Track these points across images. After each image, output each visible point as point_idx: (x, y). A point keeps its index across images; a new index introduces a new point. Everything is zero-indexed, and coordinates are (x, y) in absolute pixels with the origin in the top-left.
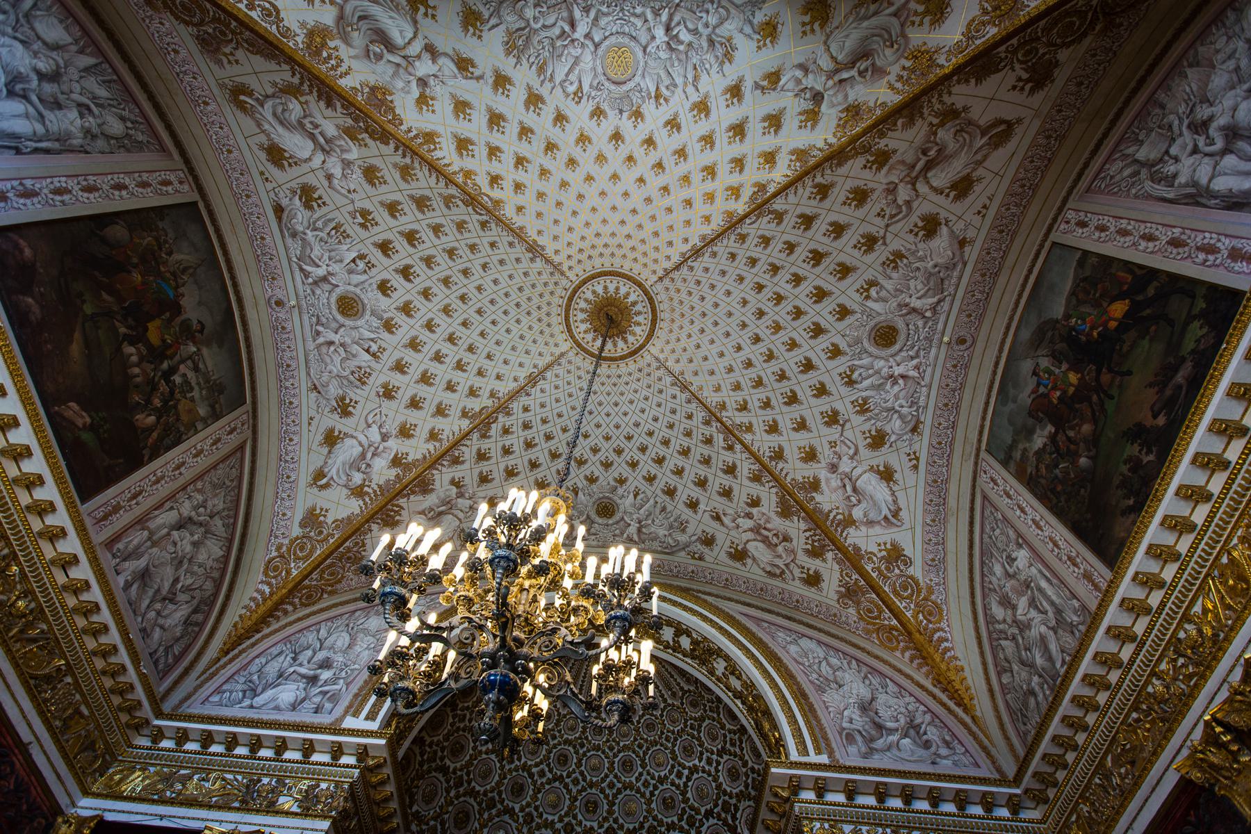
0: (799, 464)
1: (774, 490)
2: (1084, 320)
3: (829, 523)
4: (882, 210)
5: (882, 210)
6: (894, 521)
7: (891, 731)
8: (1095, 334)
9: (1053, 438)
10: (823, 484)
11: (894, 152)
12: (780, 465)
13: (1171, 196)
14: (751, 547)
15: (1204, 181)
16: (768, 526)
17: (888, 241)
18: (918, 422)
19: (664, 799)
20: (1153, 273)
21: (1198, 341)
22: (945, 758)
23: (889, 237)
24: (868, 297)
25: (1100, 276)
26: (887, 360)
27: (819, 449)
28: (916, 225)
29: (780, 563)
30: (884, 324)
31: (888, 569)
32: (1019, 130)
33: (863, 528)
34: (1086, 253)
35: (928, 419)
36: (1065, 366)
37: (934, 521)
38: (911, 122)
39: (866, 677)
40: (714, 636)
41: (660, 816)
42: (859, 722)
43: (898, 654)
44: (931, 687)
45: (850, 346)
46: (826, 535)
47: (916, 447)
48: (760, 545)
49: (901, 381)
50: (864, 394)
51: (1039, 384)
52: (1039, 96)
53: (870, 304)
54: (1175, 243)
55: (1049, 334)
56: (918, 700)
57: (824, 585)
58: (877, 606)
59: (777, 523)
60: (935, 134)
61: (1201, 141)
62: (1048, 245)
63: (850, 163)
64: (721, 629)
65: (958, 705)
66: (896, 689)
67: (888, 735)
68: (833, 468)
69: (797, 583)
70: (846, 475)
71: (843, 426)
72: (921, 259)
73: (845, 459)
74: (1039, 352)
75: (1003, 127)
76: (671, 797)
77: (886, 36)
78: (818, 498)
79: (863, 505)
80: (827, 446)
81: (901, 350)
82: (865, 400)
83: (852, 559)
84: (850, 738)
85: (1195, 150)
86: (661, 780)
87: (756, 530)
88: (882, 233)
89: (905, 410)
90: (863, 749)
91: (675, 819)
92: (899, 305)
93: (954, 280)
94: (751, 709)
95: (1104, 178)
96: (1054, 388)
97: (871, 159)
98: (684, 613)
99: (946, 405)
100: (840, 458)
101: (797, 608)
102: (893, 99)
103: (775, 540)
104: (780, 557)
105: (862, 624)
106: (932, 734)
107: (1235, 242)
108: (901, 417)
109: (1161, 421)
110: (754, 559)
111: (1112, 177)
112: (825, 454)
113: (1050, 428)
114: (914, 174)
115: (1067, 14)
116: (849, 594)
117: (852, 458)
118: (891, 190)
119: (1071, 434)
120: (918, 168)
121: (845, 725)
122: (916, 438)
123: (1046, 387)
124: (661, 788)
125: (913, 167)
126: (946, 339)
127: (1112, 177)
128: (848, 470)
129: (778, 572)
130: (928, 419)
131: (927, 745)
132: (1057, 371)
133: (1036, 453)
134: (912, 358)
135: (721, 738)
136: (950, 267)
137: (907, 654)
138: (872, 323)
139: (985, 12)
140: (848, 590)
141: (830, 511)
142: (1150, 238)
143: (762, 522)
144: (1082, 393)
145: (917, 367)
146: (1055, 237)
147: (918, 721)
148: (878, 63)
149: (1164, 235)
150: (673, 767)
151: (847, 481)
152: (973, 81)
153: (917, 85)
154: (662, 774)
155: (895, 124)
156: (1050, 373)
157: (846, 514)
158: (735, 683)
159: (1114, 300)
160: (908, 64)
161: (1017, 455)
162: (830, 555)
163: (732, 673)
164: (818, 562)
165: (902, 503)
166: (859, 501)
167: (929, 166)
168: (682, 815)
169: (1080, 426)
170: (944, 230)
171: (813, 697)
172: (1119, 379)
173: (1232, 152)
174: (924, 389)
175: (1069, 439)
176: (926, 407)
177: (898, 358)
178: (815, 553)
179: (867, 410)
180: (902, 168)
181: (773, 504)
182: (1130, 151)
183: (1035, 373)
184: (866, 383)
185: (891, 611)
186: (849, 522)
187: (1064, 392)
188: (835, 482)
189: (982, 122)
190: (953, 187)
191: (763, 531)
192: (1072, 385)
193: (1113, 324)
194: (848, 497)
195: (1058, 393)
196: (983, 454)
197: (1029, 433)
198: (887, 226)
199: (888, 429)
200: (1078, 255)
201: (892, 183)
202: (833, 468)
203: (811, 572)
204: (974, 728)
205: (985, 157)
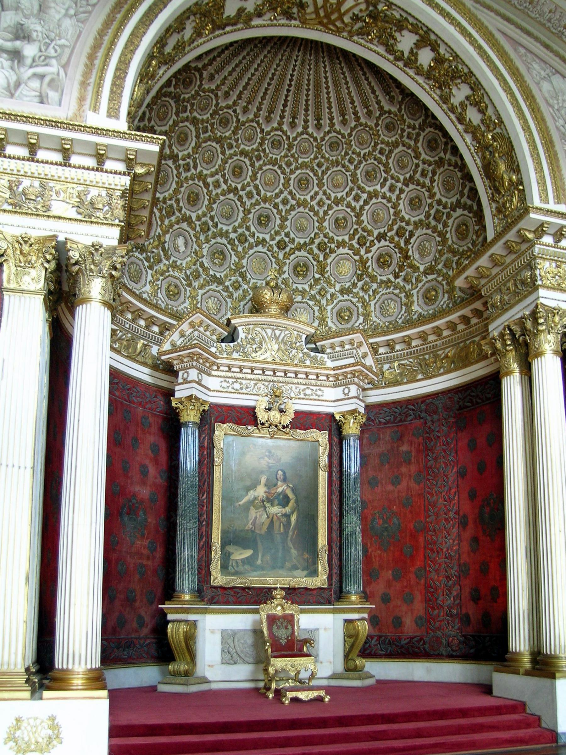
19: (337, 220)
40: (471, 58)
41: (331, 234)
64: (479, 48)
76: (345, 219)
86: (337, 202)
91: (346, 238)
94: (483, 147)
98: (440, 19)
124: (336, 208)
135: (411, 166)
150: (352, 189)
154: (339, 195)
158: (473, 115)
163: (476, 104)
168: (354, 235)
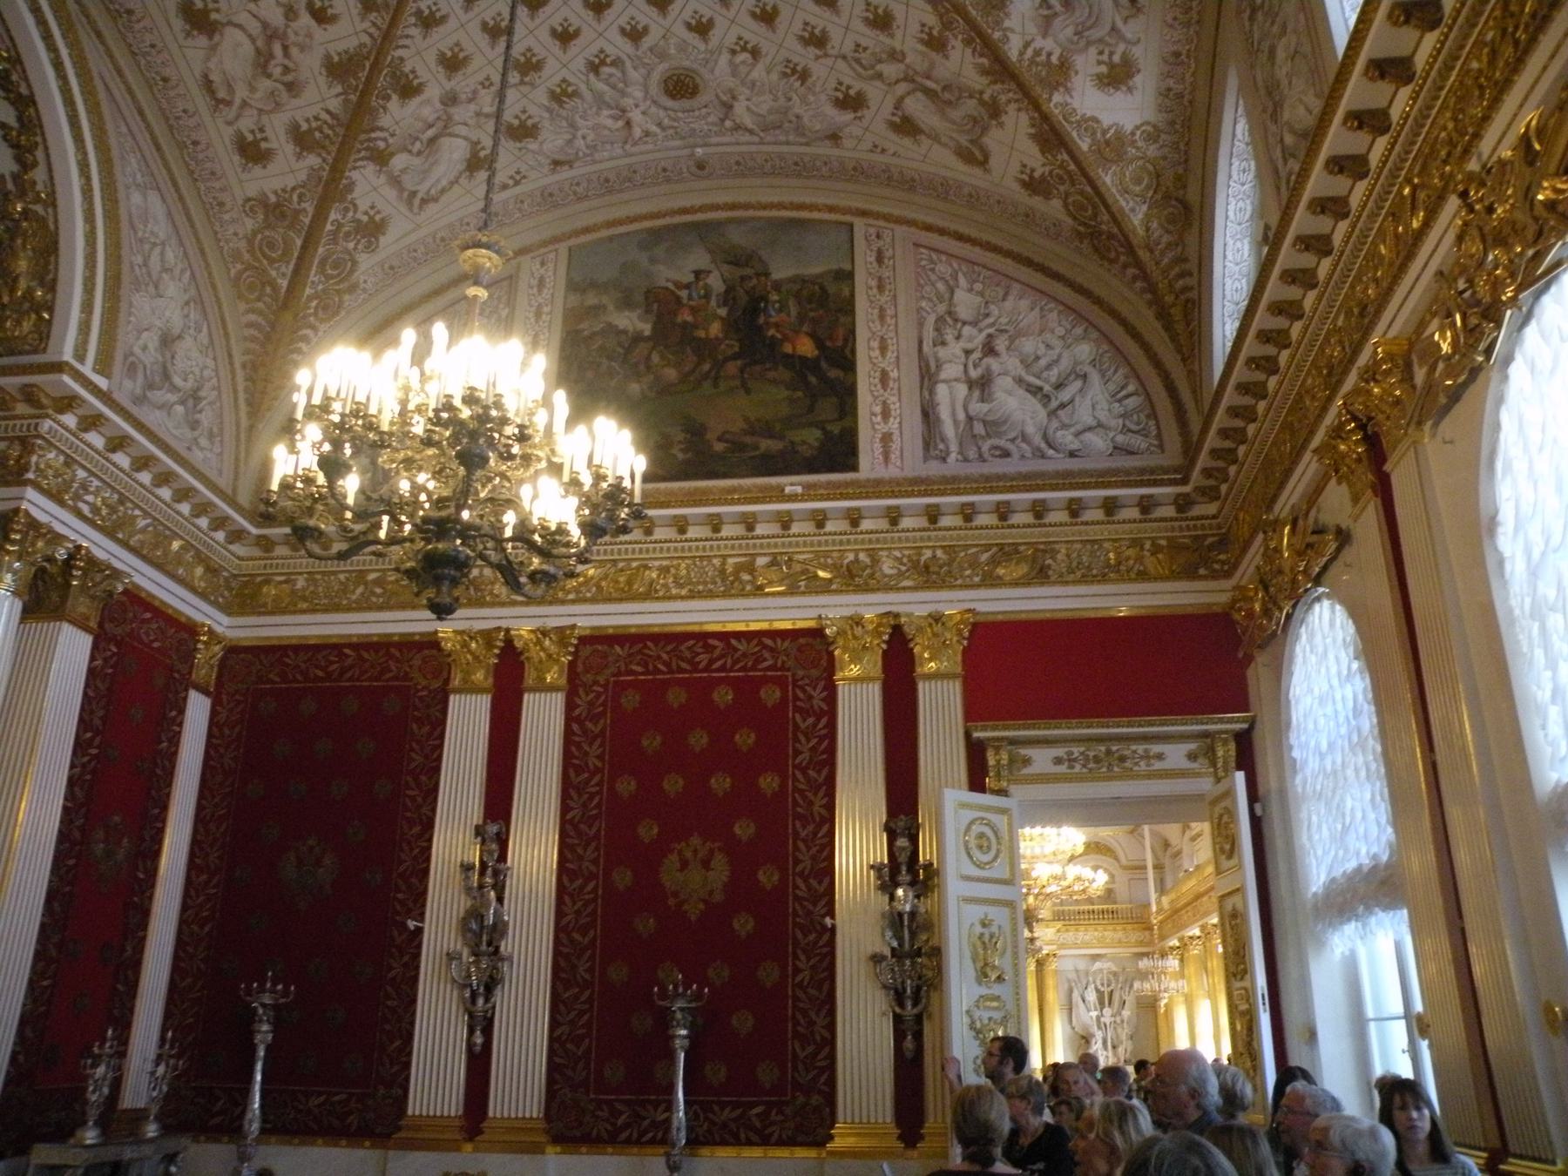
0: (431, 57)
1: (366, 39)
2: (780, 310)
3: (363, 137)
4: (865, 49)
5: (865, 49)
6: (417, 202)
7: (174, 388)
8: (771, 332)
9: (638, 338)
10: (416, 101)
11: (946, 57)
12: (414, 31)
13: (926, 348)
14: (232, 35)
15: (943, 376)
16: (294, 51)
17: (823, 61)
18: (570, 164)
20: (849, 366)
21: (804, 442)
22: (202, 449)
23: (829, 61)
24: (733, 52)
25: (829, 305)
26: (645, 98)
27: (469, 70)
28: (849, 87)
29: (241, 93)
30: (698, 80)
31: (348, 234)
32: (978, 171)
33: (383, 179)
34: (850, 276)
35: (578, 171)
36: (723, 312)
37: (443, 239)
38: (984, 72)
39: (187, 303)
42: (150, 356)
43: (242, 306)
44: (237, 365)
45: (651, 49)
46: (342, 144)
47: (533, 175)
48: (247, 49)
49: (620, 123)
50: (583, 87)
51: (687, 286)
52: (1016, 187)
53: (725, 58)
54: (884, 378)
55: (748, 271)
56: (216, 371)
57: (257, 171)
58: (286, 252)
59: (310, 65)
60: (971, 97)
61: (976, 355)
62: (848, 218)
63: (929, 8)
65: (249, 404)
66: (206, 341)
67: (169, 391)
68: (451, 100)
69: (229, 132)
70: (450, 118)
71: (522, 83)
72: (804, 100)
73: (472, 107)
74: (726, 267)
75: (980, 158)
77: (1088, 24)
78: (394, 104)
79: (416, 161)
80: (480, 77)
81: (666, 109)
82: (575, 94)
83: (332, 188)
84: (132, 369)
85: (968, 352)
87: (271, 34)
88: (831, 52)
89: (580, 143)
90: (138, 391)
92: (731, 91)
93: (782, 138)
95: (932, 261)
96: (694, 311)
97: (935, 33)
99: (607, 180)
100: (470, 101)
101: (182, 146)
102: (1013, 50)
103: (277, 71)
104: (253, 89)
105: (243, 245)
106: (206, 418)
107: (897, 432)
108: (570, 142)
109: (719, 447)
110: (213, 48)
111: (933, 270)
112: (463, 83)
113: (646, 329)
114: (919, 79)
115: (1095, 207)
116: (274, 210)
117: (478, 114)
118: (895, 56)
119: (656, 358)
120: (929, 83)
121: (137, 350)
122: (546, 170)
123: (690, 298)
125: (928, 78)
126: (699, 150)
127: (933, 270)
128: (456, 117)
129: (221, 94)
130: (578, 171)
131: (194, 425)
132: (713, 303)
133: (610, 325)
134: (659, 125)
136: (800, 129)
137: (252, 317)
138: (695, 66)
139: (1104, 132)
140: (278, 205)
141: (382, 129)
142: (883, 349)
143: (292, 37)
144: (704, 349)
145: (647, 134)
146: (859, 224)
147: (202, 394)
148: (1057, 22)
149: (887, 363)
151: (440, 124)
152: (1033, 131)
153: (1028, 78)
155: (981, 55)
156: (707, 296)
157: (391, 149)
159: (812, 335)
160: (1054, 59)
161: (591, 299)
162: (313, 160)
164: (290, 148)
165: (444, 199)
166: (419, 153)
167: (929, 93)
169: (668, 365)
170: (852, 116)
171: (124, 292)
172: (737, 383)
173: (970, 388)
174: (620, 151)
175: (648, 358)
176: (595, 162)
177: (653, 109)
178: (302, 140)
179: (560, 103)
180: (926, 64)
181: (341, 46)
182: (962, 281)
183: (698, 274)
184: (600, 86)
185: (296, 271)
186: (381, 158)
187: (695, 326)
188: (428, 113)
189: (986, 140)
190: (906, 120)
191: (277, 49)
192: (707, 330)
193: (788, 348)
194: (417, 139)
195: (689, 319)
196: (563, 248)
197: (626, 303)
198: (844, 58)
199: (544, 134)
200: (847, 267)
201: (904, 55)
202: (451, 100)
203: (264, 145)
204: (243, 436)
205: (945, 145)
